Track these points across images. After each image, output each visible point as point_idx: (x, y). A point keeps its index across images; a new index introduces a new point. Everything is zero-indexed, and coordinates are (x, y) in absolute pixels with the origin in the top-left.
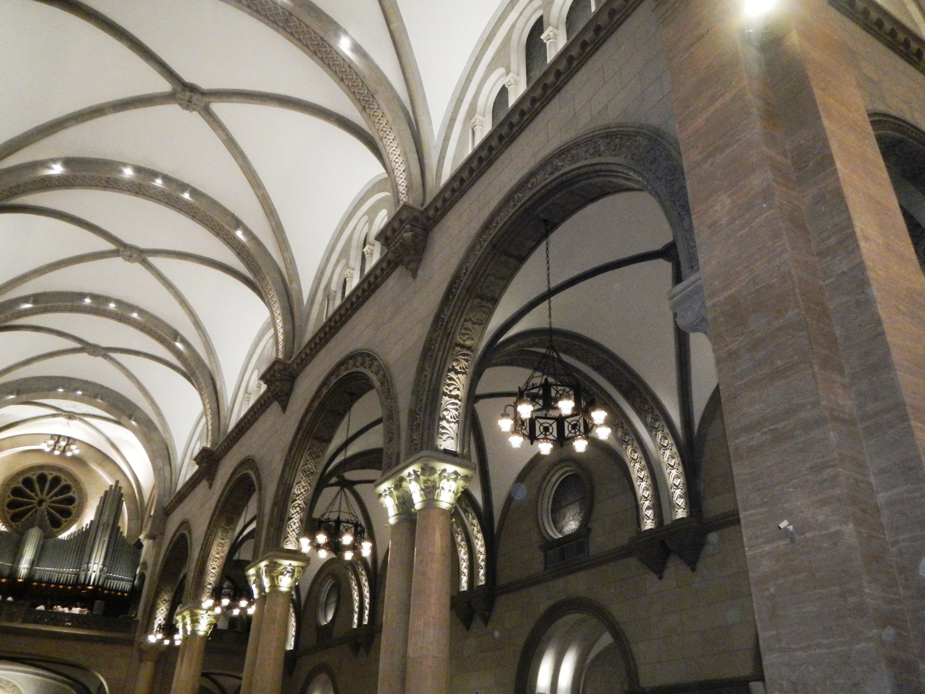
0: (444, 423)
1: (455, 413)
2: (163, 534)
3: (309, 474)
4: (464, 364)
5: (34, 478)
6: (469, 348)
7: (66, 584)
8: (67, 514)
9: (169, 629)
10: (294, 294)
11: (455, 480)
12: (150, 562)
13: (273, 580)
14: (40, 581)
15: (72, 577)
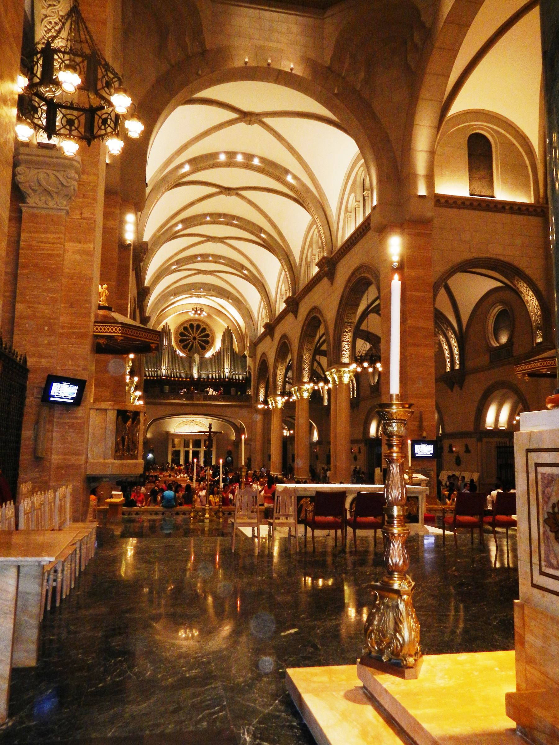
0: (344, 352)
1: (347, 347)
2: (255, 355)
3: (309, 350)
4: (349, 329)
5: (188, 326)
6: (351, 323)
7: (216, 379)
8: (207, 342)
9: (266, 402)
10: (292, 262)
11: (349, 373)
12: (252, 367)
13: (300, 394)
14: (204, 379)
15: (217, 376)
